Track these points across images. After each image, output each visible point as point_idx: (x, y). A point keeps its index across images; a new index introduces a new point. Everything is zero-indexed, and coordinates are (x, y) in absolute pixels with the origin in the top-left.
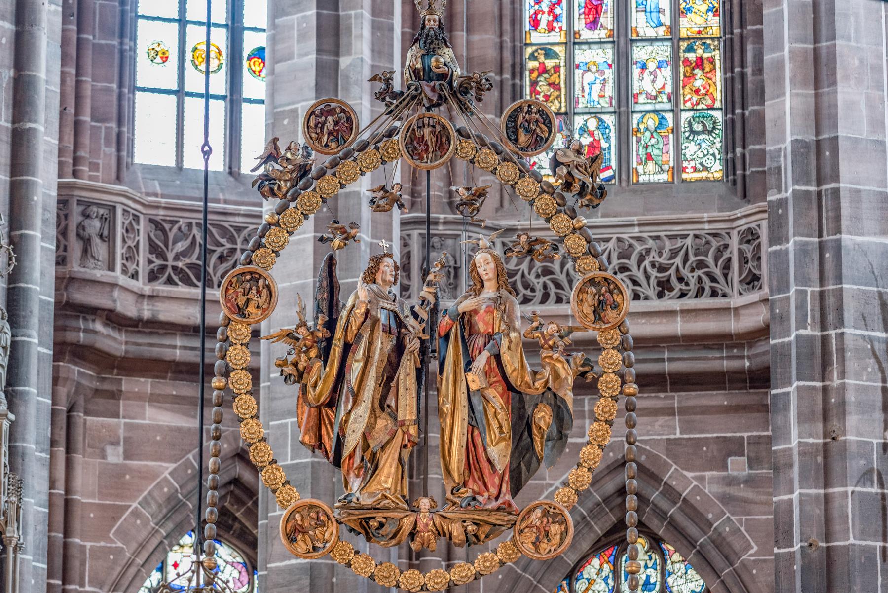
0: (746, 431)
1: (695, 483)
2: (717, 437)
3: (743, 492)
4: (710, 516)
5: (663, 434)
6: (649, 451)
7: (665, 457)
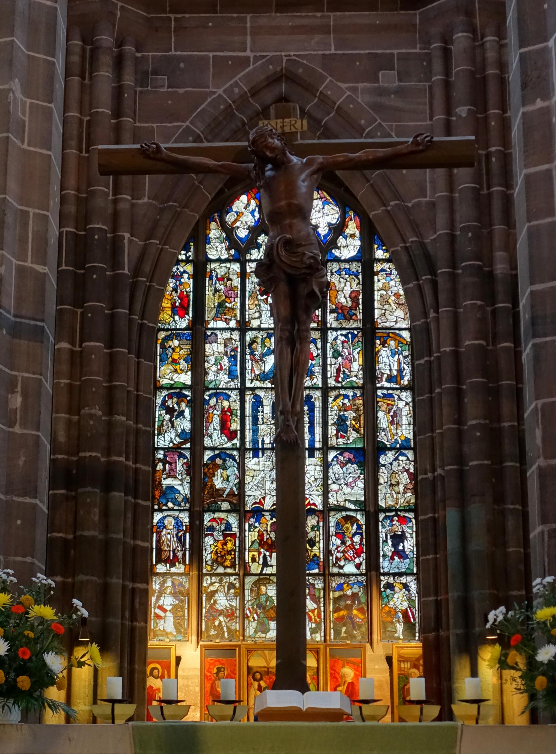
0: (396, 49)
1: (348, 93)
2: (369, 53)
3: (393, 101)
4: (363, 122)
5: (317, 50)
6: (306, 65)
7: (321, 70)
